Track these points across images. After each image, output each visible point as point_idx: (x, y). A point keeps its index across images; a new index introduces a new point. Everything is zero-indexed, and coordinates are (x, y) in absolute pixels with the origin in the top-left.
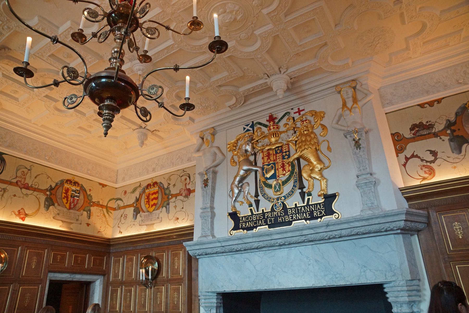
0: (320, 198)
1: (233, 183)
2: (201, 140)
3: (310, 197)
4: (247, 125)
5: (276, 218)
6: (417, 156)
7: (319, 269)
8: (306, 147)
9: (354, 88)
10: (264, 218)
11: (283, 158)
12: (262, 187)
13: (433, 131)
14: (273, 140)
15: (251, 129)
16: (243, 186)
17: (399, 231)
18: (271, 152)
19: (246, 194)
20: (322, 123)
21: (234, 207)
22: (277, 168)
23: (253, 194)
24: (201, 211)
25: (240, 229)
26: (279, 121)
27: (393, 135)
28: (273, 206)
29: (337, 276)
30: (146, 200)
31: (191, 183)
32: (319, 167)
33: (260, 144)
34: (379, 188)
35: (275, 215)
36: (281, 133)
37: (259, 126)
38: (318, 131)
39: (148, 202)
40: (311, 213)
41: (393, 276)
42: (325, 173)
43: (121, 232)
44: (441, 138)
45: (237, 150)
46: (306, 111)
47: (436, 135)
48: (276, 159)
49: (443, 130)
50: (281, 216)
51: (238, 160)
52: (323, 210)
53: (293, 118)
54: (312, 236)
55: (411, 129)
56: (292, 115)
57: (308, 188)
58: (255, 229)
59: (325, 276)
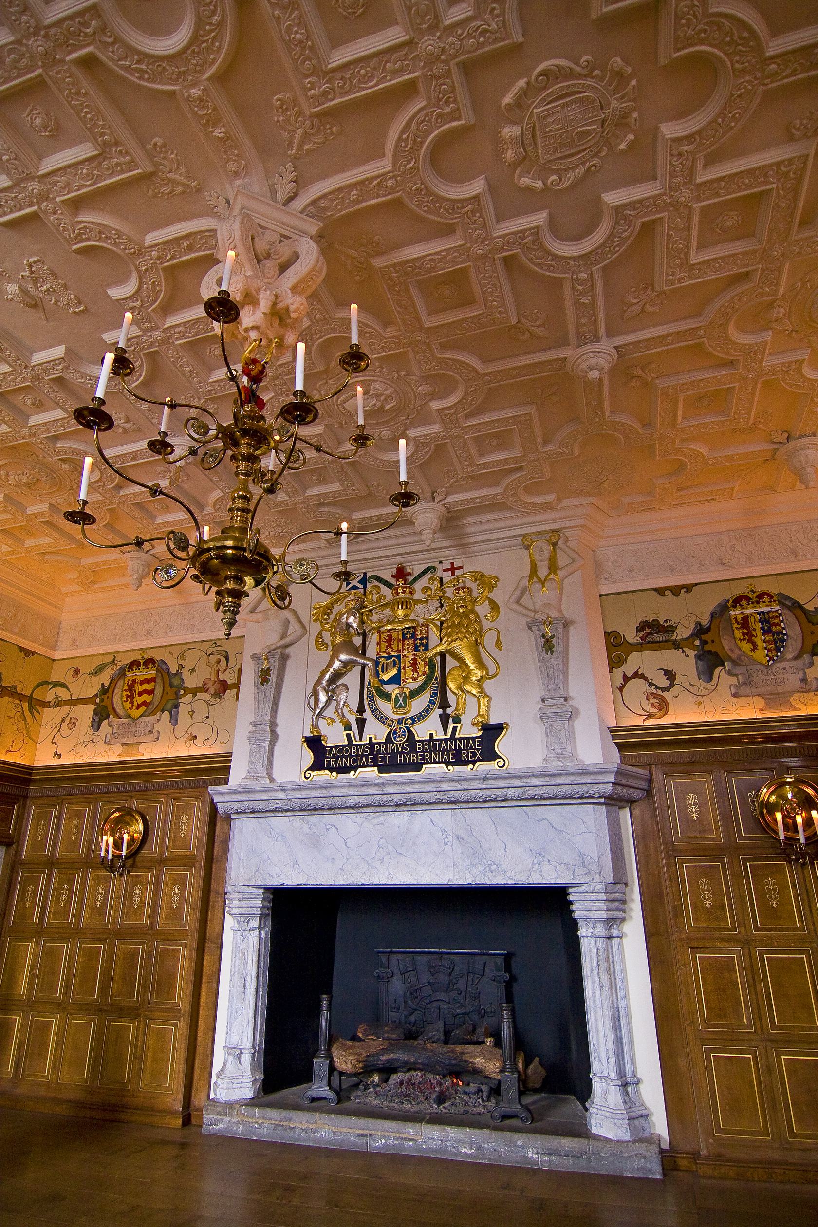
0: (476, 729)
1: (318, 682)
3: (459, 725)
5: (394, 755)
6: (643, 677)
7: (462, 853)
9: (554, 545)
10: (372, 753)
11: (416, 649)
12: (373, 697)
13: (674, 638)
14: (400, 613)
15: (361, 586)
16: (337, 691)
17: (602, 800)
18: (394, 635)
19: (341, 706)
20: (490, 595)
21: (315, 726)
22: (402, 665)
23: (355, 707)
24: (251, 728)
26: (415, 580)
27: (607, 634)
28: (390, 732)
29: (492, 868)
30: (125, 693)
32: (479, 674)
33: (375, 617)
34: (578, 724)
35: (393, 750)
37: (376, 583)
38: (483, 609)
39: (130, 698)
40: (458, 753)
41: (586, 874)
42: (488, 685)
43: (58, 755)
44: (683, 652)
45: (330, 621)
46: (466, 570)
47: (677, 645)
48: (403, 649)
49: (688, 638)
51: (332, 642)
52: (478, 750)
53: (441, 579)
54: (456, 794)
55: (639, 629)
56: (440, 573)
57: (456, 709)
58: (353, 772)
59: (472, 865)
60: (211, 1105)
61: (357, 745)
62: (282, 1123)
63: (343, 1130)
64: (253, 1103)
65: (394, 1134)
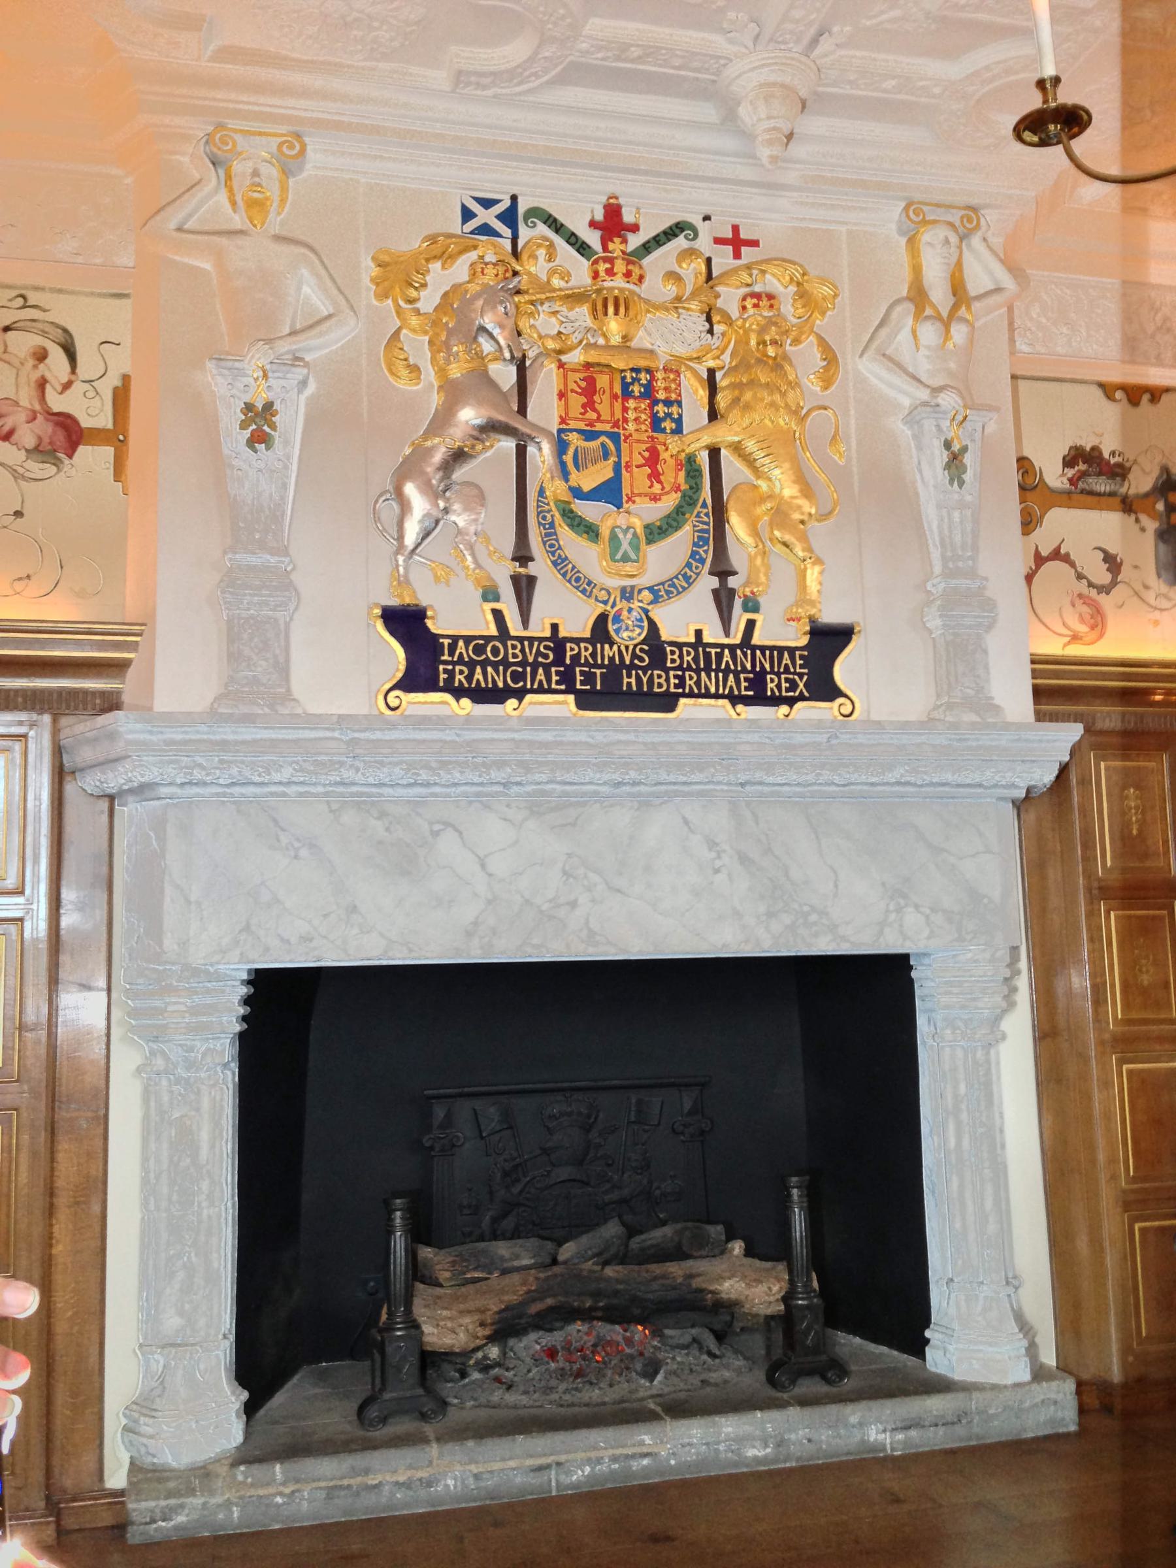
5: (614, 670)
6: (1066, 559)
10: (559, 660)
11: (656, 424)
13: (1123, 490)
15: (507, 232)
18: (602, 381)
21: (404, 582)
23: (508, 544)
26: (647, 248)
31: (78, 387)
37: (542, 229)
40: (758, 681)
44: (1137, 520)
47: (1127, 506)
49: (1147, 495)
50: (632, 666)
52: (801, 676)
53: (709, 261)
55: (1068, 462)
58: (512, 703)
59: (770, 915)
60: (148, 1480)
61: (521, 639)
62: (345, 1482)
63: (496, 1466)
65: (611, 1452)
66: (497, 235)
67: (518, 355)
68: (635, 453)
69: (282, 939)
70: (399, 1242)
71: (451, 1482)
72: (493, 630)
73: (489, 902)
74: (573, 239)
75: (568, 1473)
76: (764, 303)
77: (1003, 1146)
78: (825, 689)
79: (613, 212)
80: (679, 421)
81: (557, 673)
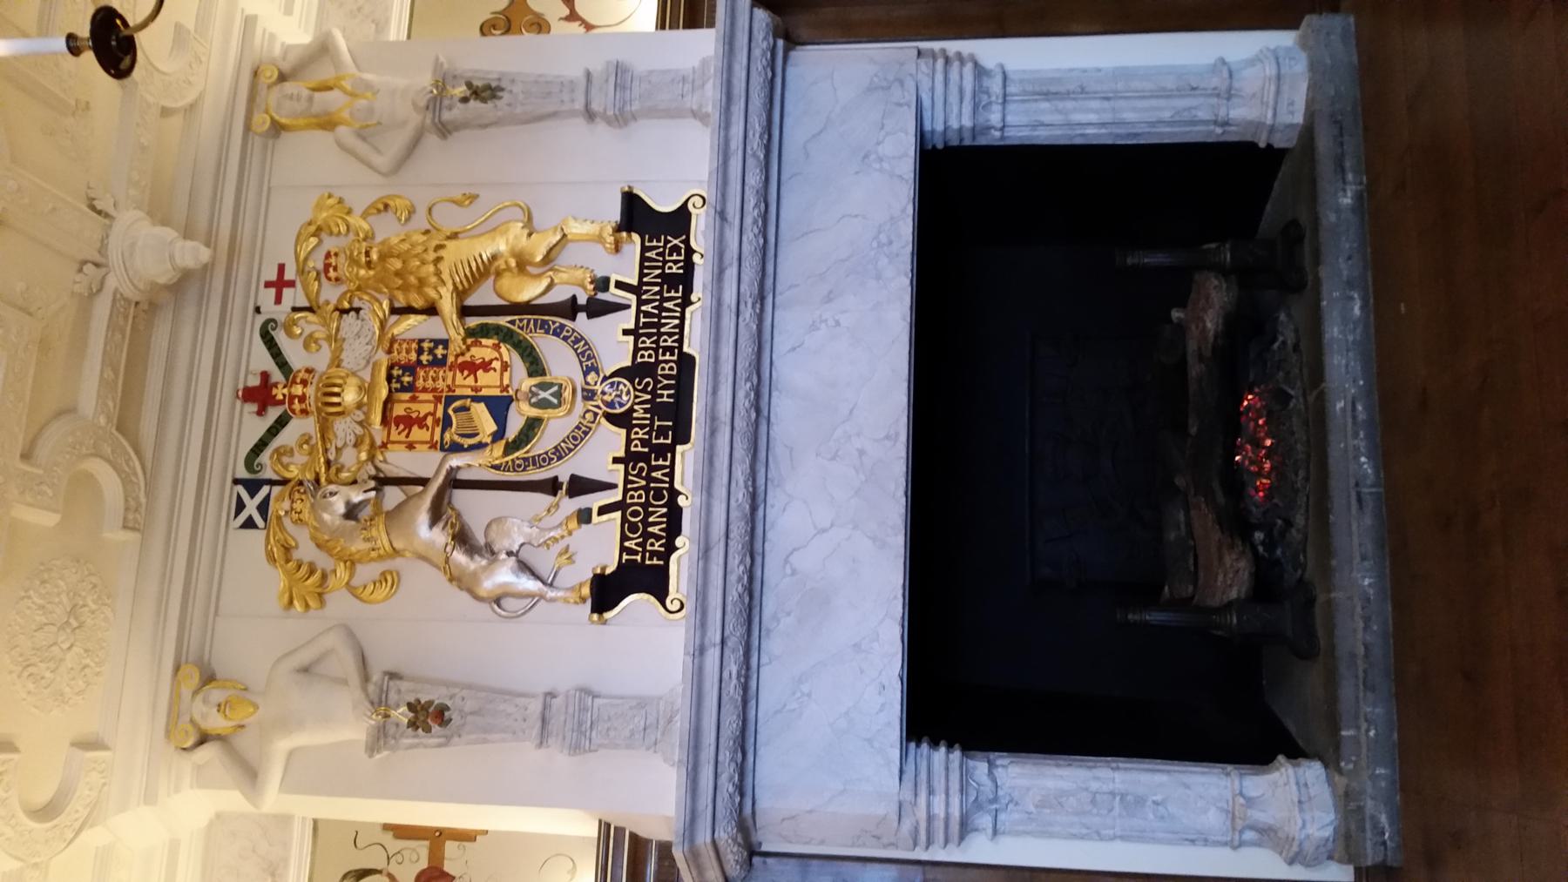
0: (626, 248)
2: (208, 752)
4: (241, 506)
5: (656, 409)
8: (431, 256)
11: (439, 363)
12: (525, 459)
15: (265, 490)
18: (398, 410)
22: (469, 392)
23: (542, 500)
25: (666, 567)
35: (646, 411)
36: (336, 362)
37: (265, 457)
40: (669, 281)
48: (434, 390)
50: (653, 393)
52: (667, 242)
53: (295, 309)
54: (745, 278)
58: (681, 501)
62: (1361, 674)
63: (1356, 541)
64: (1331, 761)
66: (269, 495)
67: (372, 484)
68: (463, 383)
69: (881, 710)
70: (1154, 617)
71: (1367, 582)
72: (618, 515)
73: (855, 527)
74: (274, 431)
75: (1365, 476)
76: (333, 261)
77: (1099, 70)
78: (680, 220)
79: (249, 395)
80: (437, 342)
81: (657, 459)
